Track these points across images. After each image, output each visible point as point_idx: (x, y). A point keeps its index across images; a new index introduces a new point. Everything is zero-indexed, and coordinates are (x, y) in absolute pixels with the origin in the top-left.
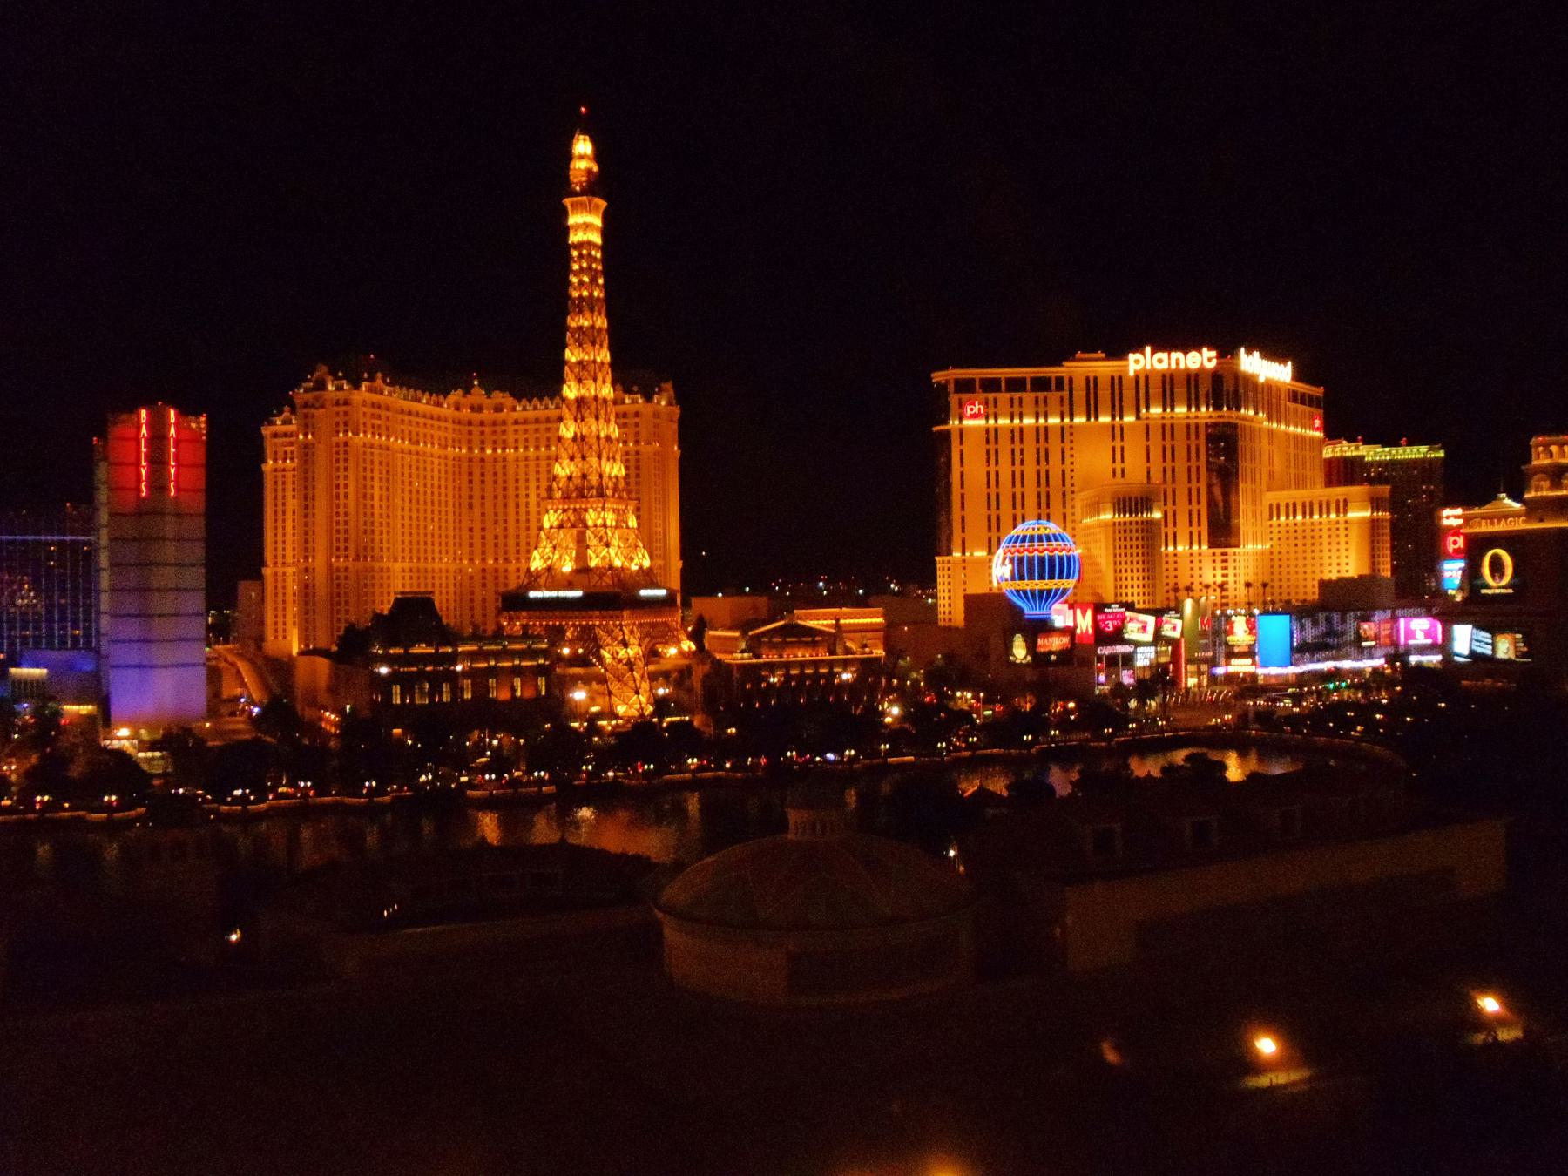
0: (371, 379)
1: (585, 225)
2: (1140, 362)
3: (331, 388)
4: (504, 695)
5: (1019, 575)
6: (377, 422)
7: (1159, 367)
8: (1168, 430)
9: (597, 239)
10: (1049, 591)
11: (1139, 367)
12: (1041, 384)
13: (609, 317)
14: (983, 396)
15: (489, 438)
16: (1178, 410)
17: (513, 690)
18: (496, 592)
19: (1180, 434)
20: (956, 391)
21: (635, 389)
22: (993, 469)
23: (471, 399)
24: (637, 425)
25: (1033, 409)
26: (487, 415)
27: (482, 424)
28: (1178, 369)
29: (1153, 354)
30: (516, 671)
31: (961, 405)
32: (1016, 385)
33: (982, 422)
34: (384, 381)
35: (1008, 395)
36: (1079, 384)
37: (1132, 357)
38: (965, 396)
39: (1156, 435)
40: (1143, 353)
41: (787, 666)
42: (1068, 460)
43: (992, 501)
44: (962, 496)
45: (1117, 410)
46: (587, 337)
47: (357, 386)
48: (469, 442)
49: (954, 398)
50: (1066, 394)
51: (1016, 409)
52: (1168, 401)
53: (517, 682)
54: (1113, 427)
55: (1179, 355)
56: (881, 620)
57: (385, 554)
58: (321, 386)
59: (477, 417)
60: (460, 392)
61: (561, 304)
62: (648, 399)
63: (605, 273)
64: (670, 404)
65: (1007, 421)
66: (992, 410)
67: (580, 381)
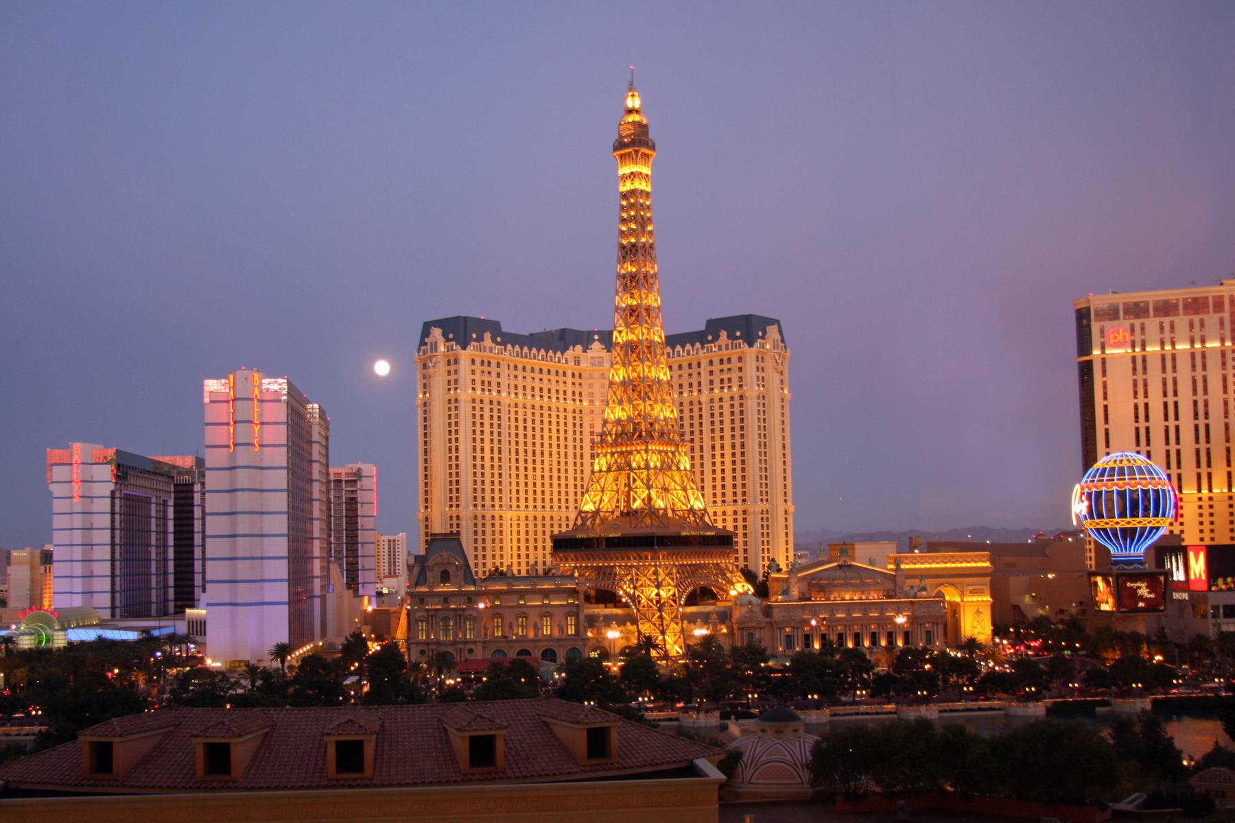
0: (480, 339)
5: (1095, 511)
6: (486, 379)
18: (551, 537)
21: (738, 334)
22: (1141, 401)
23: (590, 354)
24: (740, 369)
34: (494, 341)
35: (1158, 320)
41: (833, 608)
47: (464, 348)
49: (1095, 327)
51: (1167, 335)
56: (987, 564)
57: (497, 503)
60: (579, 348)
62: (751, 345)
66: (1138, 337)
67: (627, 326)
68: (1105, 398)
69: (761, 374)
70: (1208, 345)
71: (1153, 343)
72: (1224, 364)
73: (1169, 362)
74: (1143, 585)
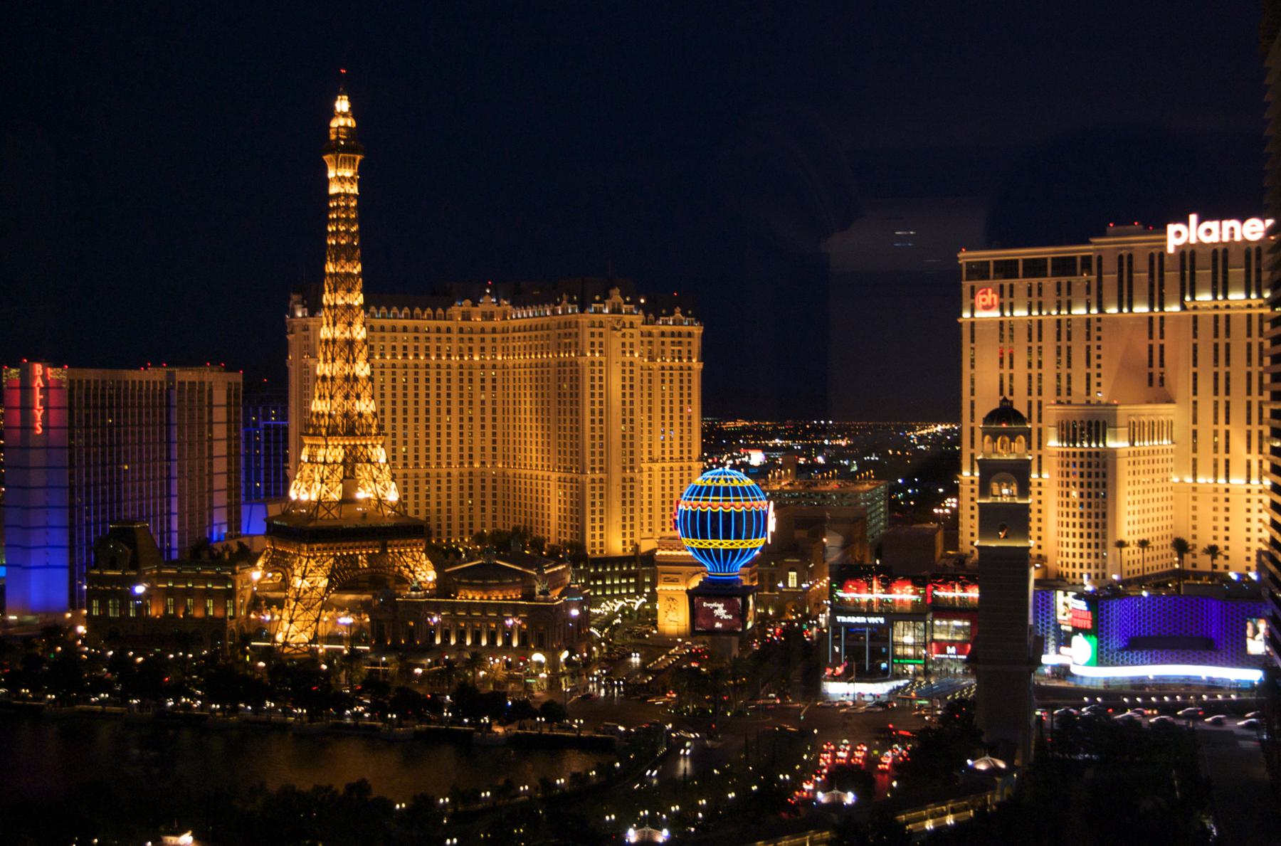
1: (342, 179)
2: (1185, 234)
3: (299, 314)
4: (199, 613)
7: (1206, 240)
8: (1223, 324)
9: (354, 190)
10: (708, 551)
11: (1181, 241)
12: (1065, 267)
13: (363, 261)
14: (997, 283)
15: (499, 345)
16: (1232, 296)
17: (207, 610)
19: (1239, 329)
20: (968, 279)
23: (481, 308)
25: (1026, 300)
26: (497, 322)
27: (494, 331)
28: (1232, 243)
29: (1200, 222)
30: (208, 594)
32: (1035, 268)
35: (1026, 282)
36: (1110, 265)
37: (1172, 228)
38: (977, 283)
39: (1206, 329)
40: (1186, 223)
42: (1094, 361)
44: (972, 403)
45: (1156, 298)
46: (343, 281)
48: (483, 349)
49: (966, 285)
50: (1094, 278)
51: (1035, 299)
52: (1221, 286)
53: (210, 603)
54: (1151, 319)
55: (1234, 223)
58: (293, 316)
59: (489, 325)
61: (319, 254)
62: (582, 311)
63: (360, 220)
64: (616, 310)
65: (1024, 313)
66: (1007, 300)
69: (597, 340)
70: (1075, 311)
71: (1021, 306)
72: (1088, 334)
73: (1035, 331)
74: (721, 606)
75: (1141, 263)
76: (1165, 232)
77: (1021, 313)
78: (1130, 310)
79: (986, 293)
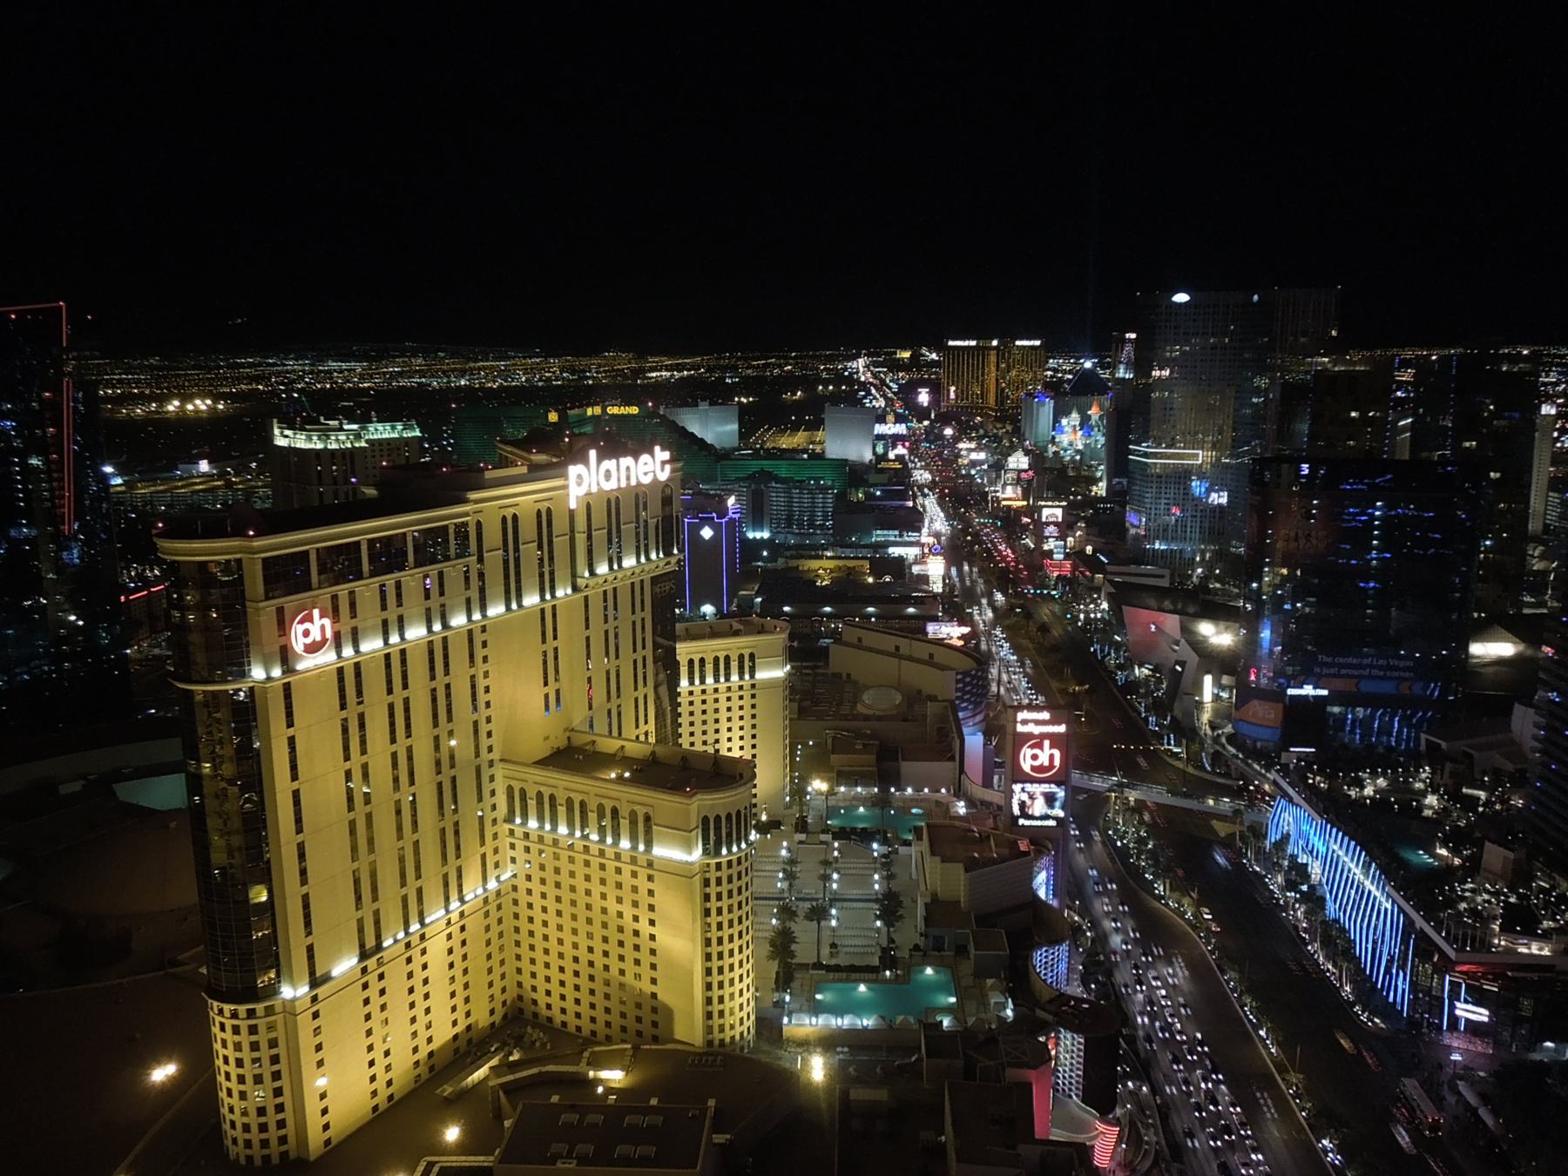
11: (582, 491)
12: (432, 548)
29: (600, 460)
31: (283, 626)
32: (389, 556)
33: (327, 657)
36: (493, 535)
37: (574, 470)
38: (289, 602)
40: (586, 462)
43: (360, 837)
55: (627, 461)
65: (378, 643)
68: (294, 777)
71: (369, 632)
72: (472, 656)
75: (528, 530)
76: (565, 476)
77: (372, 645)
78: (520, 606)
79: (311, 621)
